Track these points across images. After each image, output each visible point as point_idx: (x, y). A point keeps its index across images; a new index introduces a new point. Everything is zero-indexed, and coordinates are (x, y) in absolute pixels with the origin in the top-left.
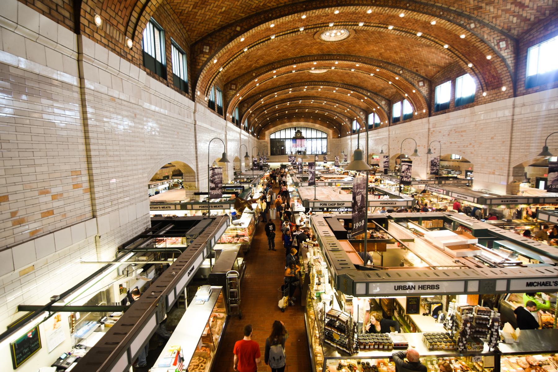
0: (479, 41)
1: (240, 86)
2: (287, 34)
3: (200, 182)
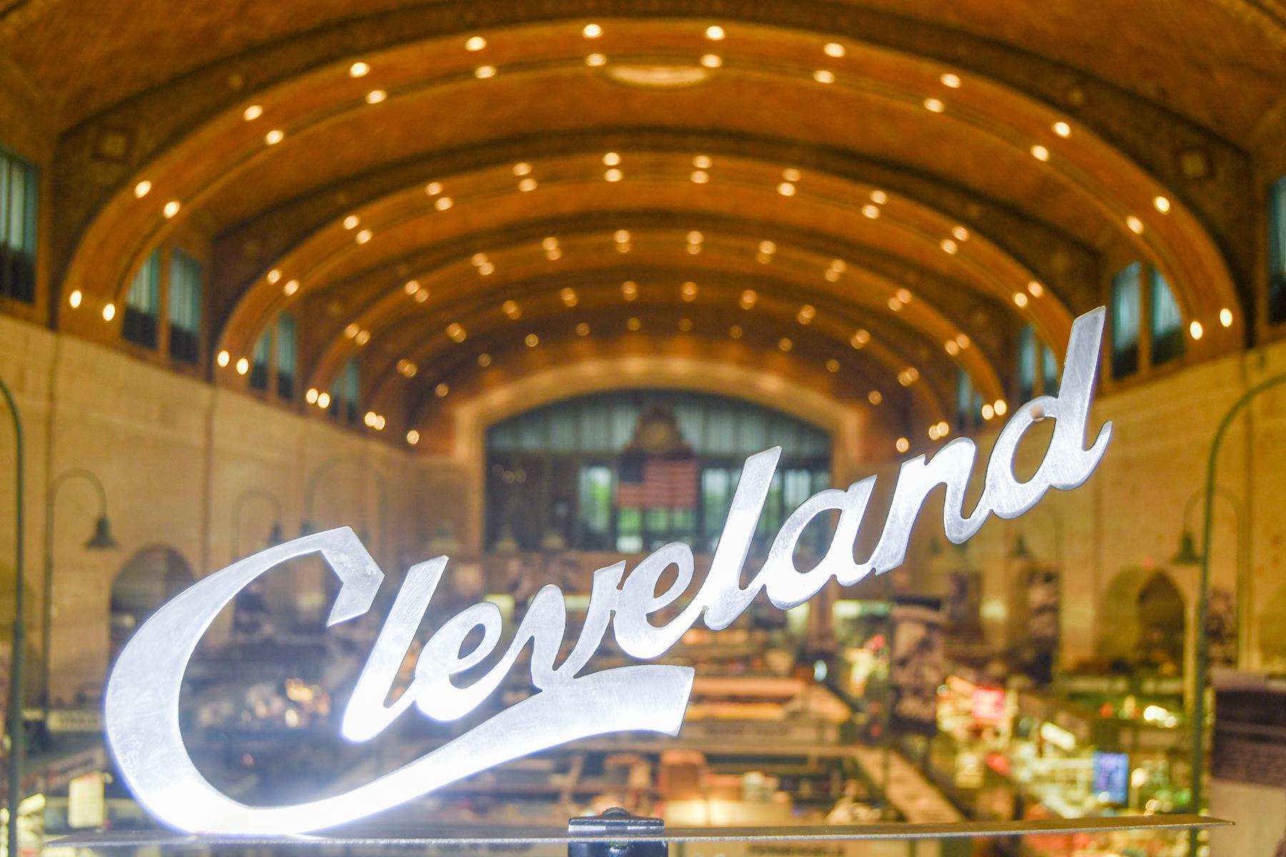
1: (150, 145)
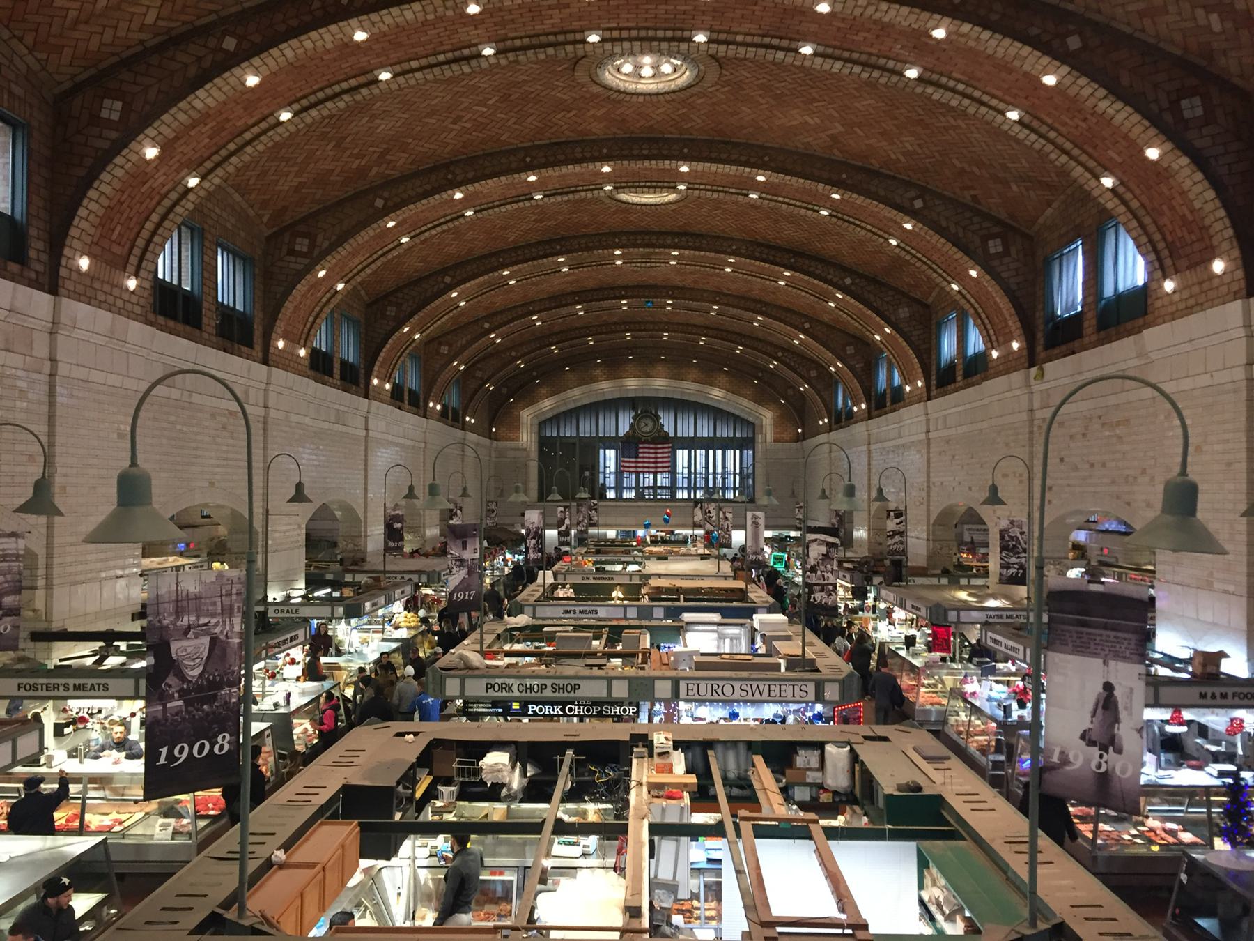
0: (1105, 97)
1: (326, 244)
2: (439, 64)
3: (57, 592)
